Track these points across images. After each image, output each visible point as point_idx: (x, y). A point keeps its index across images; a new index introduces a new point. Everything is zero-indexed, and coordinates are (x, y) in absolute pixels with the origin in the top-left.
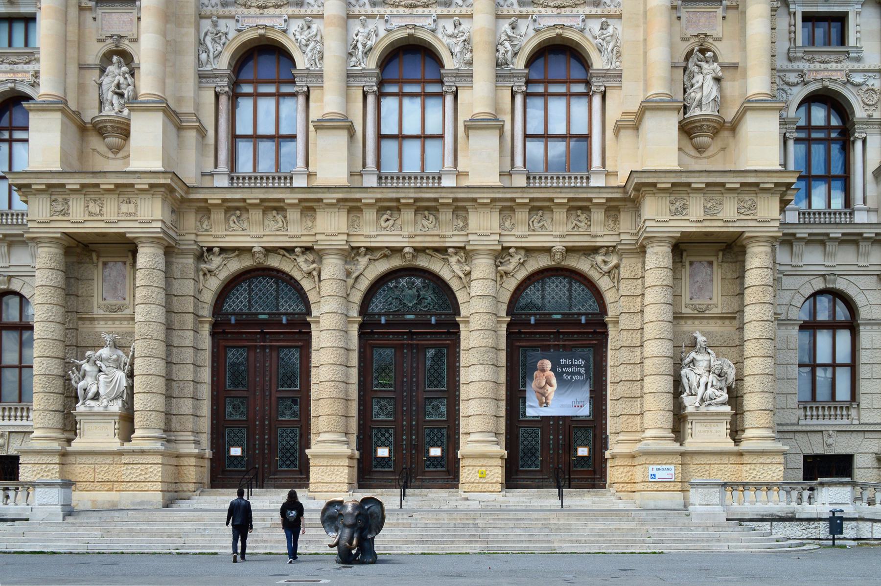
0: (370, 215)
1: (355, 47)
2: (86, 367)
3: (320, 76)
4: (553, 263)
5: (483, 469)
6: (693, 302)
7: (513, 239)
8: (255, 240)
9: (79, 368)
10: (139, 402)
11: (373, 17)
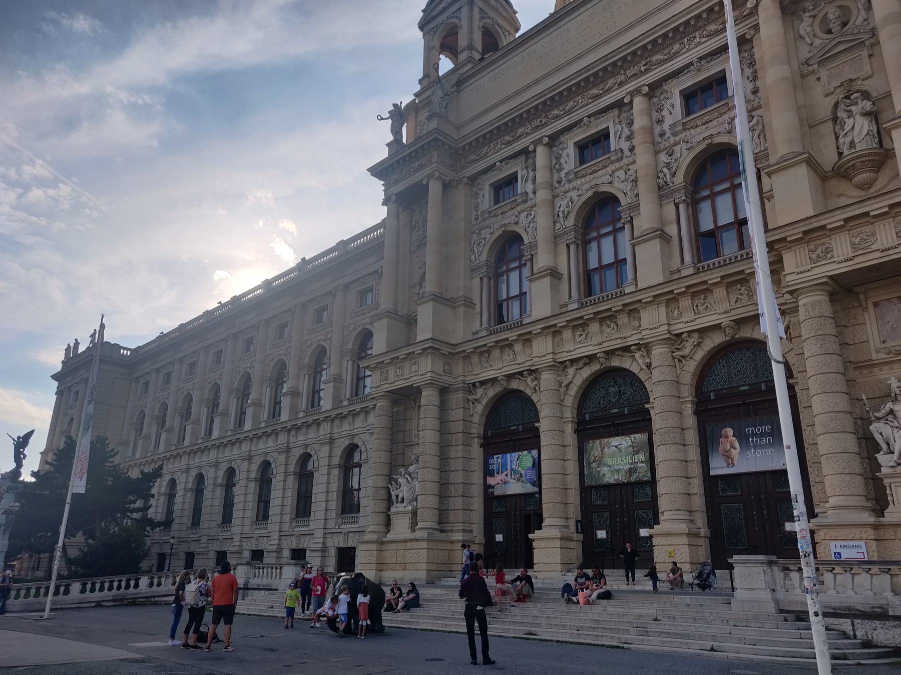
0: (567, 334)
1: (558, 216)
2: (400, 480)
4: (728, 338)
5: (672, 548)
6: (888, 344)
7: (682, 325)
8: (498, 372)
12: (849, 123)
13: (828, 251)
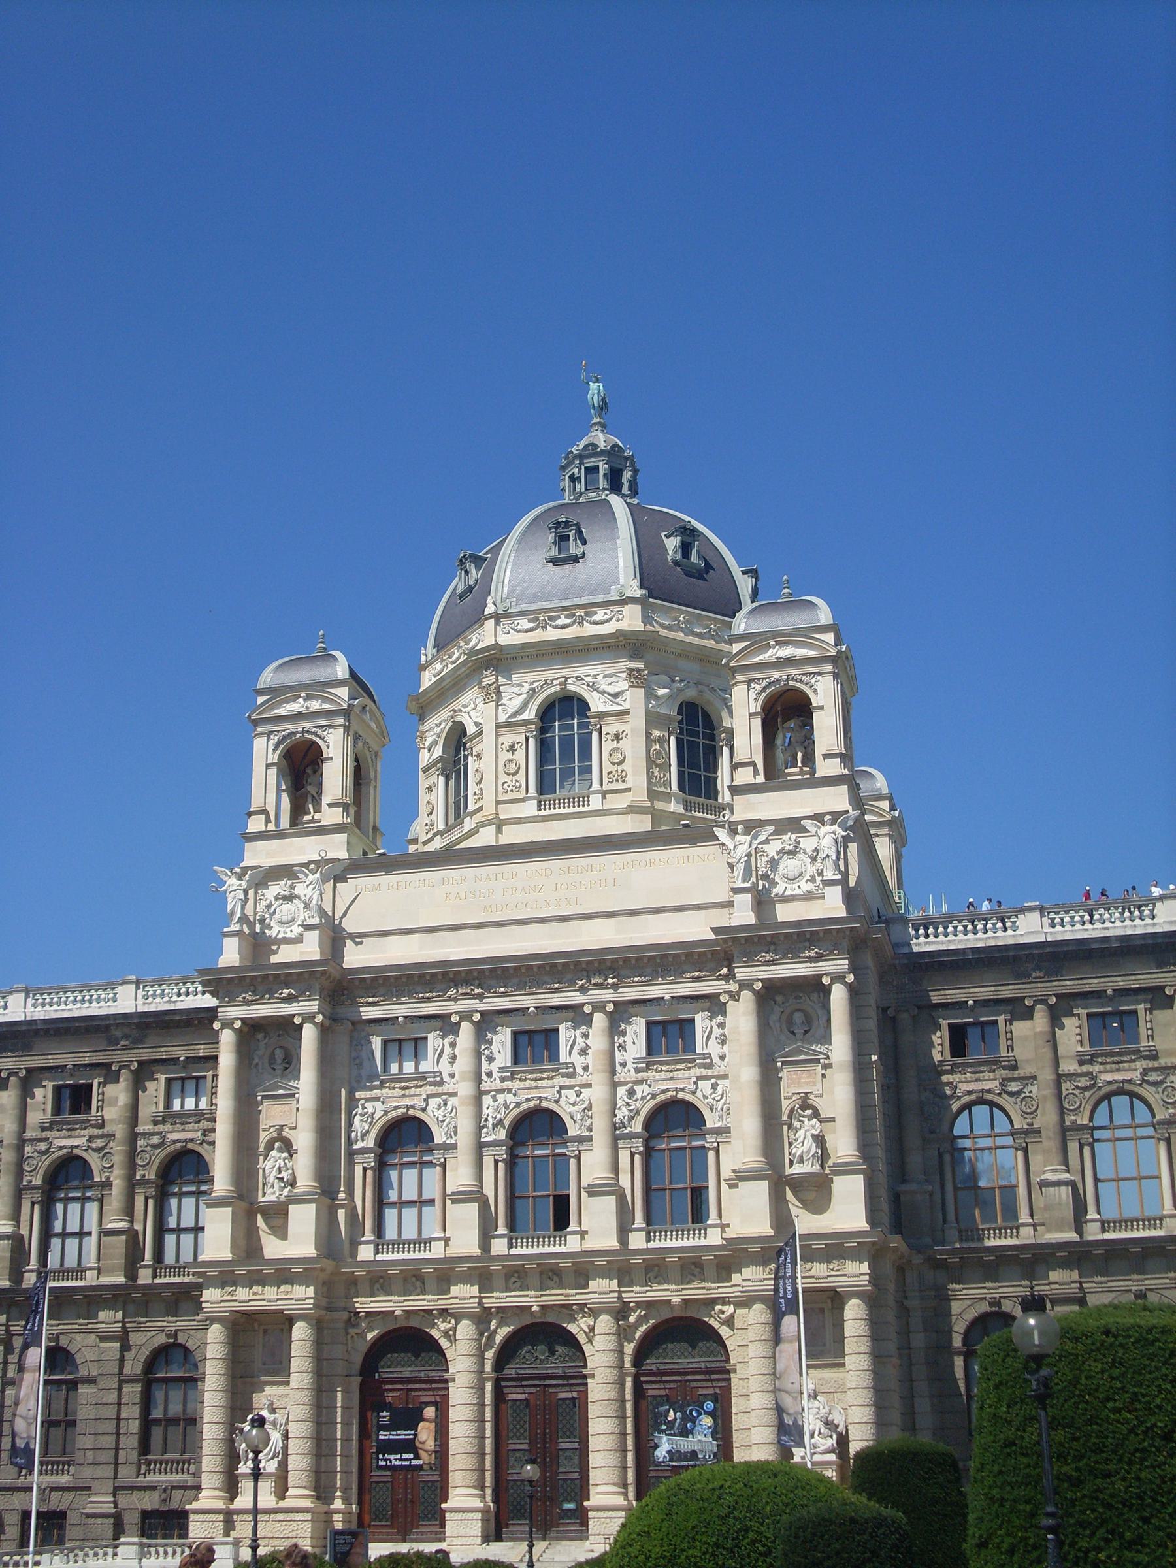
10: (293, 1462)
11: (501, 1091)
12: (801, 1133)
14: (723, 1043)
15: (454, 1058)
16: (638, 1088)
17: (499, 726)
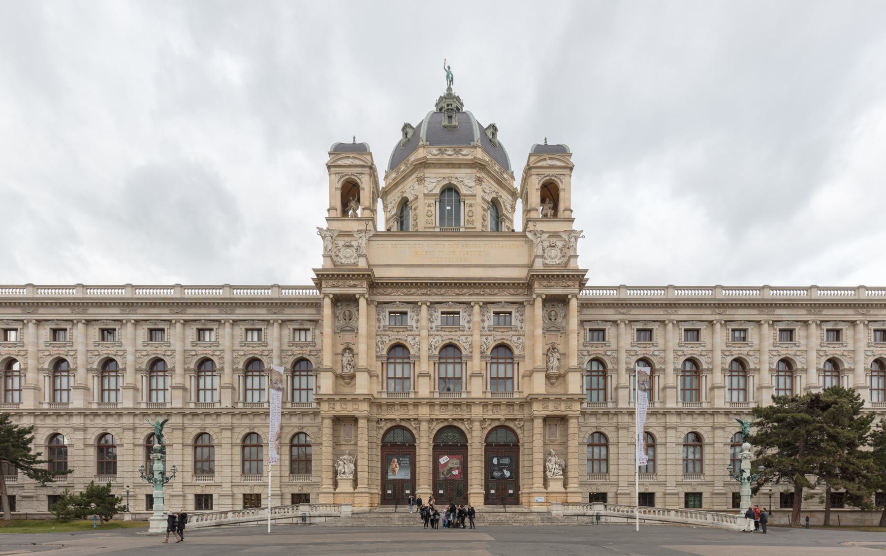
0: (437, 407)
1: (431, 346)
3: (419, 357)
9: (338, 462)
12: (552, 358)
13: (547, 406)
14: (522, 322)
15: (418, 321)
16: (490, 338)
17: (425, 195)
